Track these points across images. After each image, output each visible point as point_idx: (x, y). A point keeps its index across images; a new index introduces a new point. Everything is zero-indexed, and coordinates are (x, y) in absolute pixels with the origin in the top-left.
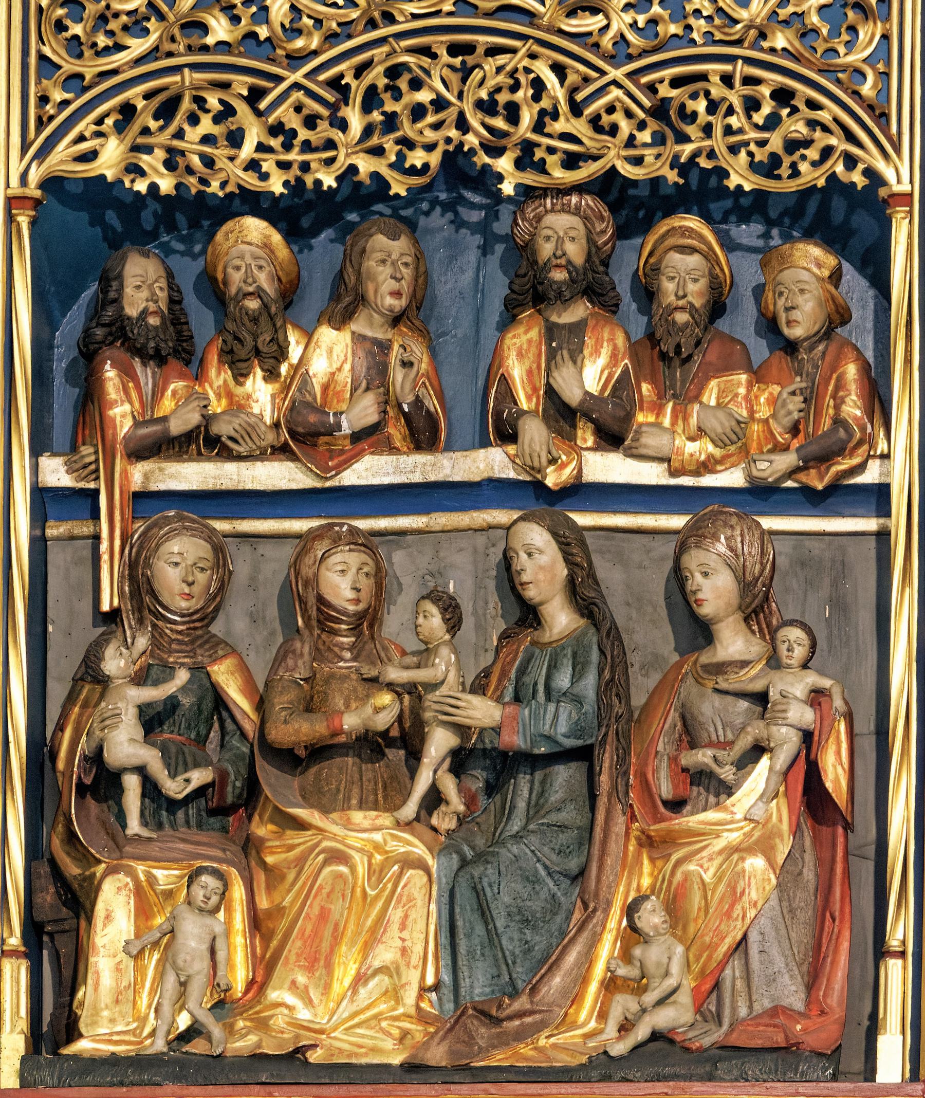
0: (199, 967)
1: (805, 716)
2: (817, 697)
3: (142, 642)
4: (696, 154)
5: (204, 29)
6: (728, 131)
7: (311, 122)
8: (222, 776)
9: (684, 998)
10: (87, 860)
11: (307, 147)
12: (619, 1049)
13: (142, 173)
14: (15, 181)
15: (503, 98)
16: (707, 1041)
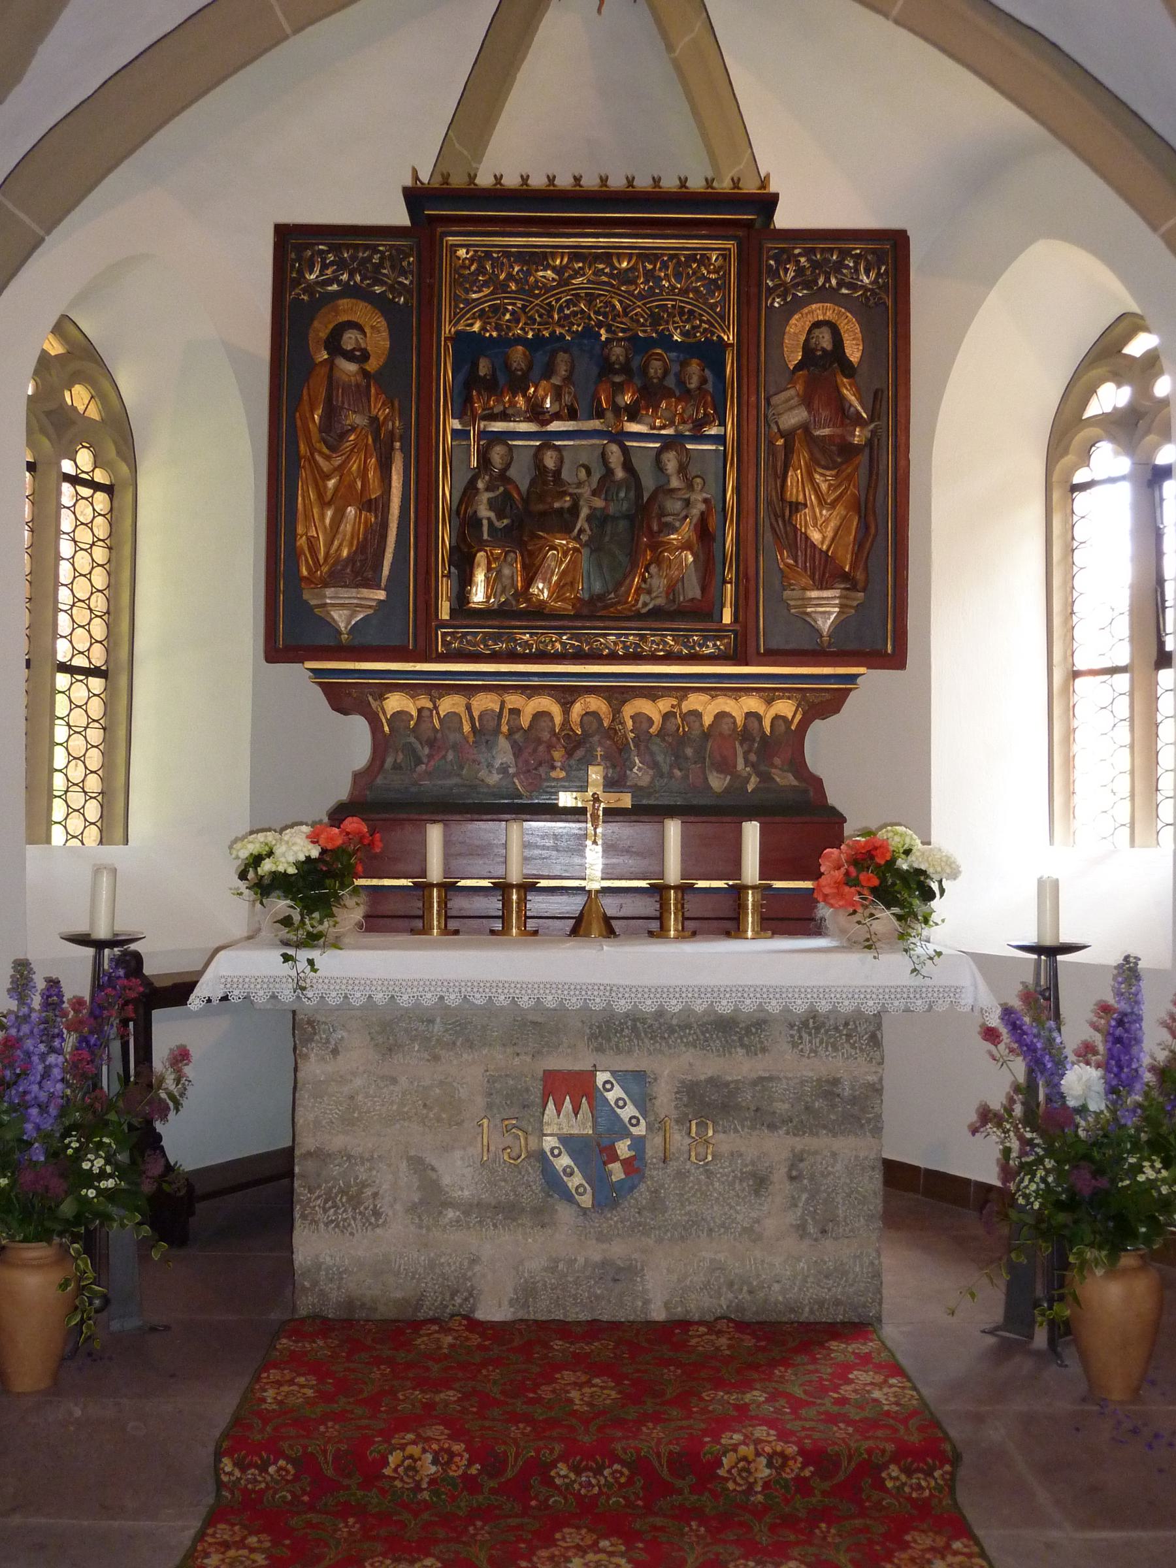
0: (507, 582)
1: (703, 507)
2: (706, 501)
3: (487, 478)
4: (663, 330)
5: (509, 286)
6: (674, 322)
7: (541, 316)
8: (513, 521)
9: (663, 595)
10: (471, 547)
11: (540, 324)
12: (644, 611)
13: (488, 331)
14: (447, 332)
15: (602, 310)
16: (672, 609)
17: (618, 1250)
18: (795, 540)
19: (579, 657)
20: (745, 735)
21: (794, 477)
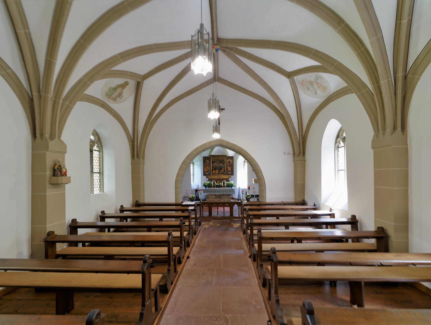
17: (220, 200)
18: (228, 170)
19: (218, 175)
20: (226, 179)
21: (228, 167)
